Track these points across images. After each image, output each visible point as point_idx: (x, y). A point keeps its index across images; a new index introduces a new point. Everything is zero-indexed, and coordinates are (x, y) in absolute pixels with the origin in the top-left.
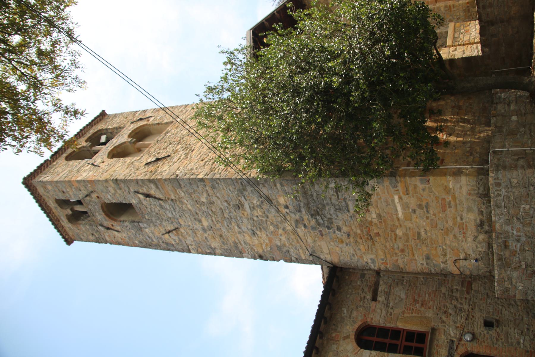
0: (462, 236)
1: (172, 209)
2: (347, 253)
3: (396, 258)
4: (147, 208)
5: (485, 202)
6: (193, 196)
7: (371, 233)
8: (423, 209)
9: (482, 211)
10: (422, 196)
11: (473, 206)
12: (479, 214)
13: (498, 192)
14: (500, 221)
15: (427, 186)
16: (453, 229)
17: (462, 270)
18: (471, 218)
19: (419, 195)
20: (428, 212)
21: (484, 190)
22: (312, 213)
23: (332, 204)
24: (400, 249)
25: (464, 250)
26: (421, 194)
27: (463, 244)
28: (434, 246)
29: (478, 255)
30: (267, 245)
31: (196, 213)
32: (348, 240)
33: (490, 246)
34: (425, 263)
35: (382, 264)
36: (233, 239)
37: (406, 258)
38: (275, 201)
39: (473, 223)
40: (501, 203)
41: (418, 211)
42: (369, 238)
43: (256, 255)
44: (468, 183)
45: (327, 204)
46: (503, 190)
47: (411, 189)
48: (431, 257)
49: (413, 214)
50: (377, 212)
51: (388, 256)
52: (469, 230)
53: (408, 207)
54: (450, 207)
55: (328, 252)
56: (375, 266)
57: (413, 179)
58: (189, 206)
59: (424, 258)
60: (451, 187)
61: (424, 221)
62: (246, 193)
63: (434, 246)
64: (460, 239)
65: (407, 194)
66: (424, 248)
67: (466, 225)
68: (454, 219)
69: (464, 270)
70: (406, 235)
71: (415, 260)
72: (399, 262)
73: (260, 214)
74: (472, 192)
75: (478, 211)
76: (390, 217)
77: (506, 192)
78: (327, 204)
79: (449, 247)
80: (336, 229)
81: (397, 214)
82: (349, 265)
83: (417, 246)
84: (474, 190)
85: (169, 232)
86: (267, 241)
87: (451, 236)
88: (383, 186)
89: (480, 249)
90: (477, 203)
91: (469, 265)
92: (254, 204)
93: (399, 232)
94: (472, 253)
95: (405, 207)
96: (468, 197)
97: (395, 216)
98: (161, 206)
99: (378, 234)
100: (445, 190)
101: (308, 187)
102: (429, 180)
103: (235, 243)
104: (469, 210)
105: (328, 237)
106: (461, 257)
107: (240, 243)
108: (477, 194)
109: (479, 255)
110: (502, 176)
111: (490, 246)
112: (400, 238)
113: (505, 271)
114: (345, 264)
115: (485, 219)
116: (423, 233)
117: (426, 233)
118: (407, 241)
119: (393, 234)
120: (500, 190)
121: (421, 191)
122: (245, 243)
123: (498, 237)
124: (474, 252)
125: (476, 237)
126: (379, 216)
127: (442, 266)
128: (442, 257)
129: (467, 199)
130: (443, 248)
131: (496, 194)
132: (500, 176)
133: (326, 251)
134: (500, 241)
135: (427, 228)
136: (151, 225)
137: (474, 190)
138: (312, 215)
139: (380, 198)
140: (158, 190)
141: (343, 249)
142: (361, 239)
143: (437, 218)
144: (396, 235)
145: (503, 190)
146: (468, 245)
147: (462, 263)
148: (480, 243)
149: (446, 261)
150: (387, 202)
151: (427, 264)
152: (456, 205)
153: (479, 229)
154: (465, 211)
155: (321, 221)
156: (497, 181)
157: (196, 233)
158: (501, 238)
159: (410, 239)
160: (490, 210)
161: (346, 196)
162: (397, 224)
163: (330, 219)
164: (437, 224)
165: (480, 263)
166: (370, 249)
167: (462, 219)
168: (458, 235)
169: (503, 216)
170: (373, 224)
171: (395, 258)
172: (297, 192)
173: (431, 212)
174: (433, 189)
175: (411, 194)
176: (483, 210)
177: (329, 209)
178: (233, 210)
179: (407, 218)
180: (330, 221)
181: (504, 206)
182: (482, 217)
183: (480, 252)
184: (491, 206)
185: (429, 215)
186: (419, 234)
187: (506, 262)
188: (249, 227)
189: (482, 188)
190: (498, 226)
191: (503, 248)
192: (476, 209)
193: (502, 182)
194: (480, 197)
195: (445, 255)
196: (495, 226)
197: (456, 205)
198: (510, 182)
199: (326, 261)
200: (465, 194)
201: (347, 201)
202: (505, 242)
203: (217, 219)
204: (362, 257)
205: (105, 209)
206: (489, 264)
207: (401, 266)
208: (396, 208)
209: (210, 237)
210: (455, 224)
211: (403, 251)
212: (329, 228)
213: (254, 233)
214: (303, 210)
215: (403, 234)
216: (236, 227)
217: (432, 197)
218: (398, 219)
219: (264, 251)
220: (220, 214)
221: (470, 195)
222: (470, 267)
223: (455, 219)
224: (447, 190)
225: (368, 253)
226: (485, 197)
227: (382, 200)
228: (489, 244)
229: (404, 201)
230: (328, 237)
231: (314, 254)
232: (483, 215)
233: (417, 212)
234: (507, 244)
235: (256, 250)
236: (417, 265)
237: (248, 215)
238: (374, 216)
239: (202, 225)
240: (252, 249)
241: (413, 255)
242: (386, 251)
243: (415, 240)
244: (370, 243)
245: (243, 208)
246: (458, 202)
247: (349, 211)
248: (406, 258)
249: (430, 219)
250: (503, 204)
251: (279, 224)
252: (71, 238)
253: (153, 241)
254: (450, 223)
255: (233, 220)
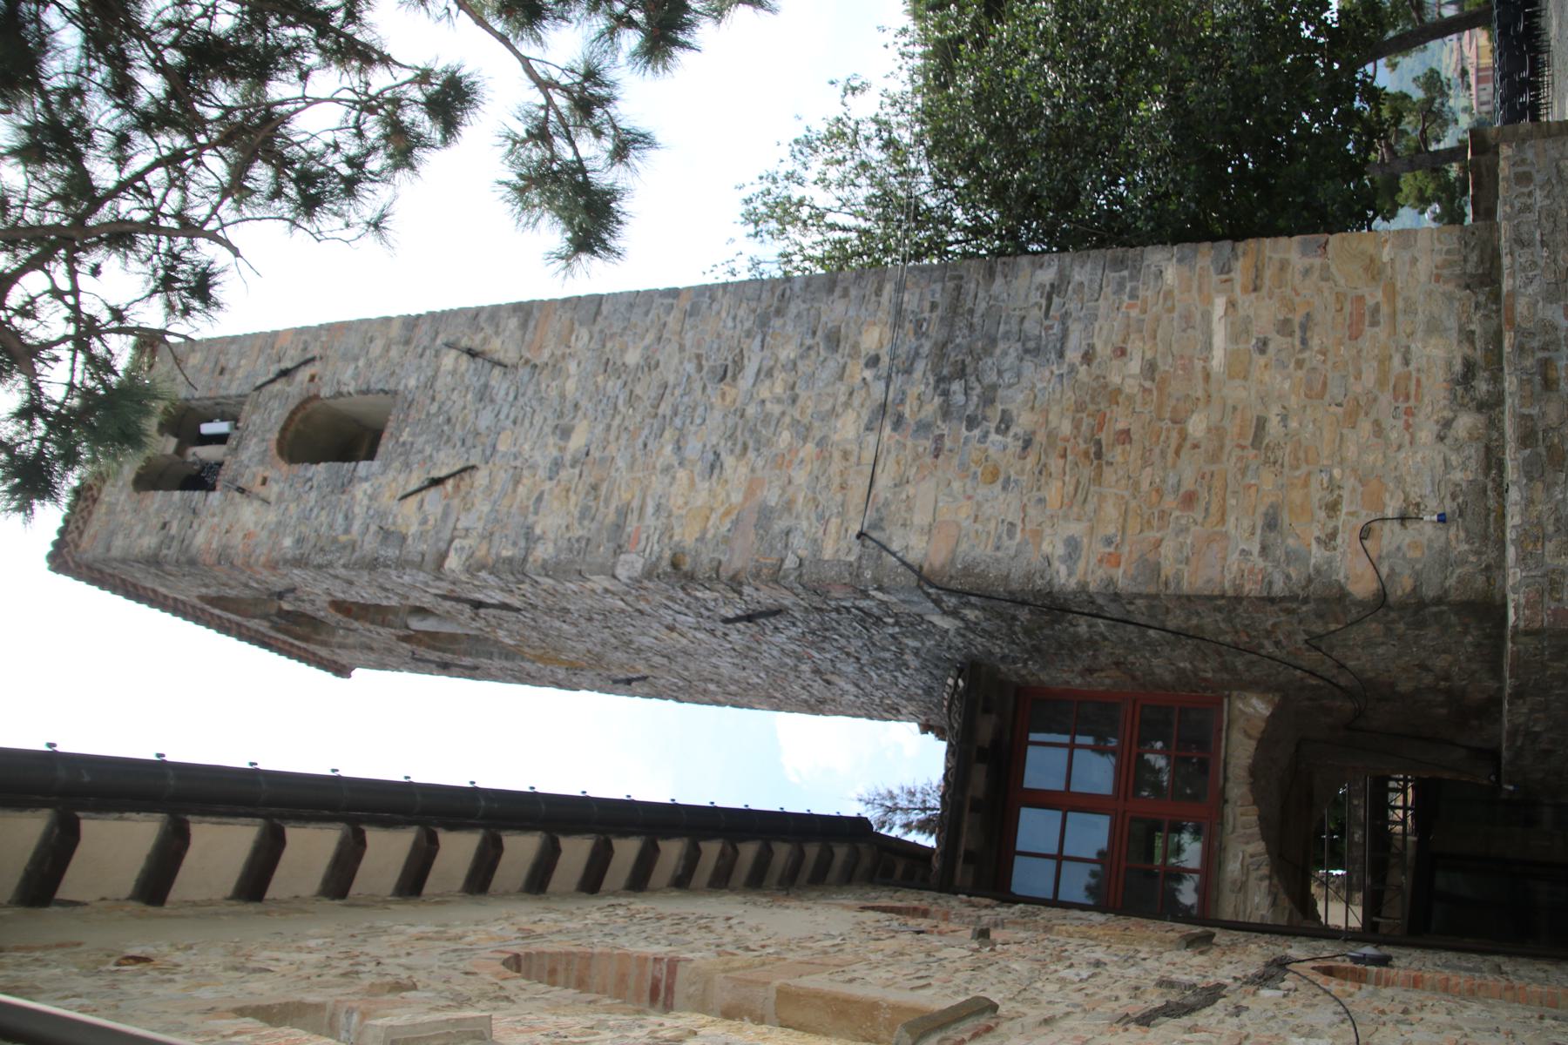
0: (1400, 423)
1: (511, 397)
2: (992, 525)
3: (1159, 535)
4: (433, 399)
5: (1482, 298)
6: (609, 345)
7: (1103, 436)
8: (1291, 334)
9: (1473, 332)
10: (1298, 295)
11: (1444, 316)
12: (1460, 342)
13: (1523, 200)
14: (1530, 290)
15: (1317, 262)
16: (1375, 399)
17: (1384, 571)
18: (1436, 356)
19: (1288, 291)
20: (1304, 342)
21: (1481, 261)
22: (945, 372)
23: (1022, 338)
24: (1182, 491)
25: (1399, 480)
26: (1294, 290)
27: (1401, 455)
28: (1304, 469)
29: (1448, 502)
30: (727, 513)
31: (576, 406)
32: (1018, 465)
33: (1492, 461)
34: (1256, 549)
35: (1101, 561)
36: (626, 496)
37: (1193, 529)
38: (851, 341)
39: (1440, 375)
40: (1533, 233)
41: (1277, 342)
42: (1093, 450)
43: (667, 554)
44: (1437, 246)
45: (1006, 336)
46: (1538, 192)
47: (1268, 274)
48: (1285, 518)
49: (1256, 356)
50: (1149, 355)
51: (1134, 525)
52: (1426, 400)
53: (1247, 332)
54: (1375, 323)
55: (928, 519)
56: (1070, 575)
57: (1283, 240)
58: (570, 386)
59: (1259, 524)
60: (1385, 258)
61: (1289, 376)
62: (777, 323)
63: (1304, 469)
64: (1393, 435)
65: (1255, 289)
66: (1268, 481)
67: (1418, 381)
68: (1381, 362)
69: (1392, 570)
70: (1217, 431)
71: (1225, 536)
72: (1162, 550)
73: (779, 389)
74: (1446, 272)
75: (1460, 331)
76: (1184, 368)
77: (1547, 197)
78: (1006, 336)
79: (1354, 470)
80: (993, 426)
81: (1206, 360)
82: (979, 576)
83: (1244, 475)
84: (1451, 264)
85: (436, 482)
86: (736, 498)
87: (1365, 426)
88: (1192, 268)
89: (1458, 476)
90: (1457, 304)
91: (1414, 545)
92: (777, 360)
93: (1197, 426)
94: (1427, 491)
95: (1238, 332)
96: (1433, 286)
97: (1198, 365)
98: (484, 395)
99: (1125, 436)
100: (1366, 269)
101: (973, 286)
102: (1327, 242)
103: (623, 512)
104: (1434, 327)
105: (956, 461)
106: (1390, 513)
107: (642, 509)
108: (1459, 277)
109: (1454, 497)
110: (1536, 155)
111: (1492, 461)
112: (1196, 446)
113: (1548, 488)
114: (967, 571)
115: (1478, 355)
116: (1274, 426)
117: (1284, 419)
118: (1214, 457)
119: (1174, 435)
120: (1530, 194)
121: (1298, 278)
122: (658, 507)
123: (1521, 349)
124: (1437, 485)
125: (1447, 424)
126: (1150, 368)
127: (1317, 554)
128: (1323, 514)
129: (1430, 294)
130: (1331, 478)
131: (1517, 205)
132: (1529, 155)
133: (921, 518)
134: (1529, 362)
135: (1293, 402)
136: (397, 464)
137: (1451, 264)
138: (940, 380)
139: (1171, 310)
140: (518, 334)
141: (986, 506)
142: (1064, 456)
143: (1330, 364)
144: (1183, 436)
145: (1538, 192)
146: (1419, 457)
147: (1391, 537)
148: (1458, 448)
149: (1333, 536)
150: (1187, 318)
151: (1264, 549)
152: (1393, 315)
153: (1459, 390)
154: (1419, 335)
155: (959, 398)
156: (1520, 169)
157: (517, 482)
158: (1533, 351)
159: (1228, 444)
160: (1495, 322)
161: (1072, 306)
162: (1200, 393)
163: (994, 387)
164: (1325, 384)
165: (1453, 530)
166: (1080, 497)
167: (1406, 363)
168: (1388, 422)
169: (1538, 272)
170: (1121, 400)
171: (1154, 535)
172: (934, 306)
173: (1315, 343)
174: (1333, 269)
175: (1264, 291)
176: (1473, 327)
177: (1005, 353)
178: (698, 386)
179: (1238, 369)
180: (988, 399)
181: (1542, 241)
182: (1467, 350)
183: (1458, 485)
184: (1498, 311)
185: (1306, 355)
186: (1261, 424)
187: (1549, 448)
188: (714, 440)
189: (1474, 257)
190: (1521, 306)
191: (1538, 388)
192: (1452, 323)
193: (1534, 172)
194: (1468, 287)
195: (1333, 508)
196: (1512, 308)
197: (1393, 315)
198: (1557, 166)
199: (904, 563)
200: (1423, 278)
201: (1070, 322)
202: (1545, 364)
203: (626, 423)
204: (1038, 534)
205: (289, 435)
206: (1485, 538)
207: (1168, 569)
208: (1209, 335)
209: (557, 491)
210: (1381, 382)
211: (1189, 500)
212: (972, 423)
213: (715, 465)
214: (920, 366)
215: (1209, 430)
216: (668, 449)
217: (1326, 294)
218: (1207, 377)
219: (701, 539)
220: (647, 403)
221: (1437, 281)
222: (1417, 554)
223: (1384, 360)
224: (1374, 270)
225: (1066, 517)
226: (1482, 284)
227: (1176, 315)
228: (1488, 449)
229: (1241, 312)
230: (956, 461)
231: (874, 535)
232: (1472, 343)
233: (1272, 347)
234: (1552, 374)
235: (676, 538)
236: (1224, 559)
237: (734, 401)
238: (1135, 366)
239: (562, 449)
240: (668, 530)
241: (1223, 519)
242: (1133, 504)
243: (1243, 448)
244: (1087, 472)
245: (734, 378)
246: (1400, 304)
247: (1061, 355)
248: (1193, 529)
249: (1307, 365)
250: (1538, 236)
251: (816, 424)
252: (77, 546)
253: (347, 531)
254: (1369, 377)
255: (678, 422)
